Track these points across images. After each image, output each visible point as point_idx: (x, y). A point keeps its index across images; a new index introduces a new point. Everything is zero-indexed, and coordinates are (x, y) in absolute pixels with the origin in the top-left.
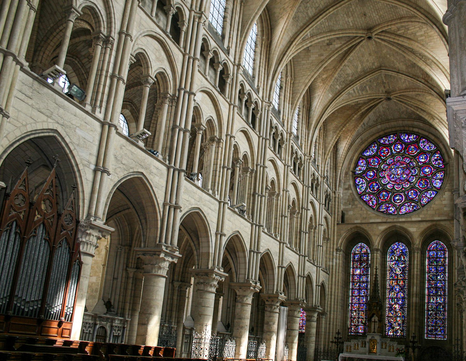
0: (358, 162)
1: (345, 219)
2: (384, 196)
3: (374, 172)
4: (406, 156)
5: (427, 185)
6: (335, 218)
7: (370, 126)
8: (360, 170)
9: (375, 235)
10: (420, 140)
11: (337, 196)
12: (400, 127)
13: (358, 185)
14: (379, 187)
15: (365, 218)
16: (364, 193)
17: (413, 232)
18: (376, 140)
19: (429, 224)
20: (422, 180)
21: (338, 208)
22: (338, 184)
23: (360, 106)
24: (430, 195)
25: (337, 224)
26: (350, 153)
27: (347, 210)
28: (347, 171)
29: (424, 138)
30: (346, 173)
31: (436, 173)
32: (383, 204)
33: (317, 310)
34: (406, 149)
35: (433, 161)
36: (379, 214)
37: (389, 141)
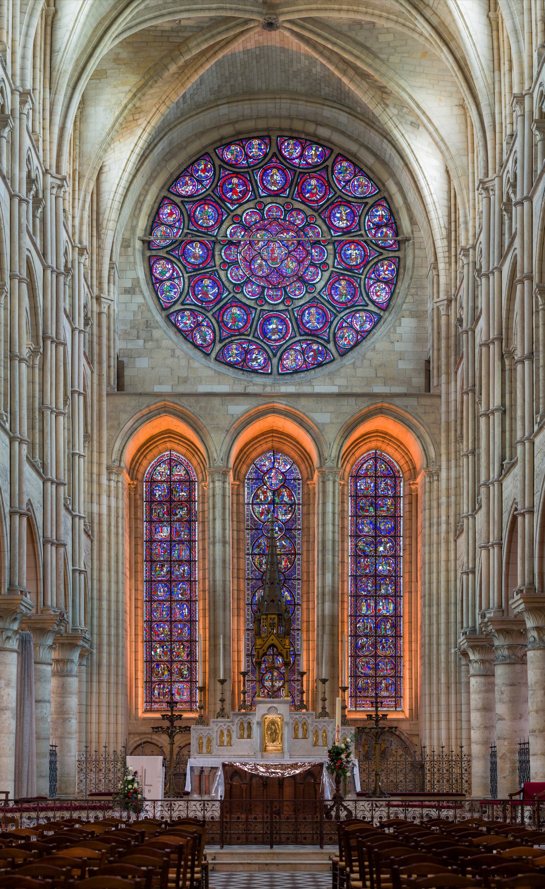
0: (158, 213)
1: (127, 380)
2: (235, 320)
3: (206, 245)
4: (297, 205)
5: (354, 296)
6: (100, 375)
7: (198, 106)
8: (166, 236)
9: (217, 428)
10: (334, 163)
11: (105, 310)
12: (280, 117)
13: (161, 281)
14: (219, 294)
15: (185, 380)
16: (178, 307)
17: (323, 424)
18: (210, 150)
19: (363, 405)
20: (338, 280)
21: (109, 347)
22: (105, 273)
23: (186, 34)
24: (361, 326)
25: (107, 394)
26: (139, 181)
27: (132, 355)
28: (127, 235)
29: (347, 160)
30: (126, 244)
31: (376, 263)
32: (232, 342)
33: (81, 643)
34: (297, 184)
35: (370, 229)
36: (223, 369)
37: (247, 156)
